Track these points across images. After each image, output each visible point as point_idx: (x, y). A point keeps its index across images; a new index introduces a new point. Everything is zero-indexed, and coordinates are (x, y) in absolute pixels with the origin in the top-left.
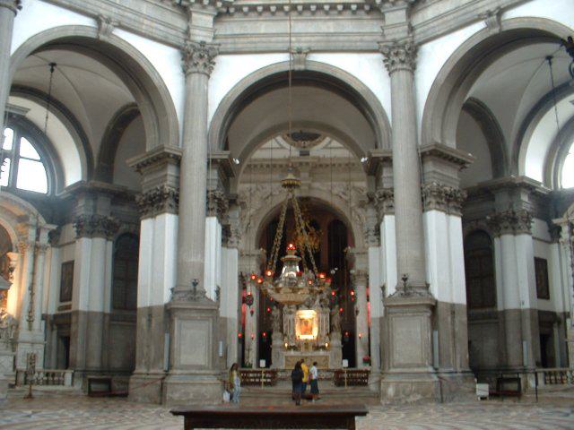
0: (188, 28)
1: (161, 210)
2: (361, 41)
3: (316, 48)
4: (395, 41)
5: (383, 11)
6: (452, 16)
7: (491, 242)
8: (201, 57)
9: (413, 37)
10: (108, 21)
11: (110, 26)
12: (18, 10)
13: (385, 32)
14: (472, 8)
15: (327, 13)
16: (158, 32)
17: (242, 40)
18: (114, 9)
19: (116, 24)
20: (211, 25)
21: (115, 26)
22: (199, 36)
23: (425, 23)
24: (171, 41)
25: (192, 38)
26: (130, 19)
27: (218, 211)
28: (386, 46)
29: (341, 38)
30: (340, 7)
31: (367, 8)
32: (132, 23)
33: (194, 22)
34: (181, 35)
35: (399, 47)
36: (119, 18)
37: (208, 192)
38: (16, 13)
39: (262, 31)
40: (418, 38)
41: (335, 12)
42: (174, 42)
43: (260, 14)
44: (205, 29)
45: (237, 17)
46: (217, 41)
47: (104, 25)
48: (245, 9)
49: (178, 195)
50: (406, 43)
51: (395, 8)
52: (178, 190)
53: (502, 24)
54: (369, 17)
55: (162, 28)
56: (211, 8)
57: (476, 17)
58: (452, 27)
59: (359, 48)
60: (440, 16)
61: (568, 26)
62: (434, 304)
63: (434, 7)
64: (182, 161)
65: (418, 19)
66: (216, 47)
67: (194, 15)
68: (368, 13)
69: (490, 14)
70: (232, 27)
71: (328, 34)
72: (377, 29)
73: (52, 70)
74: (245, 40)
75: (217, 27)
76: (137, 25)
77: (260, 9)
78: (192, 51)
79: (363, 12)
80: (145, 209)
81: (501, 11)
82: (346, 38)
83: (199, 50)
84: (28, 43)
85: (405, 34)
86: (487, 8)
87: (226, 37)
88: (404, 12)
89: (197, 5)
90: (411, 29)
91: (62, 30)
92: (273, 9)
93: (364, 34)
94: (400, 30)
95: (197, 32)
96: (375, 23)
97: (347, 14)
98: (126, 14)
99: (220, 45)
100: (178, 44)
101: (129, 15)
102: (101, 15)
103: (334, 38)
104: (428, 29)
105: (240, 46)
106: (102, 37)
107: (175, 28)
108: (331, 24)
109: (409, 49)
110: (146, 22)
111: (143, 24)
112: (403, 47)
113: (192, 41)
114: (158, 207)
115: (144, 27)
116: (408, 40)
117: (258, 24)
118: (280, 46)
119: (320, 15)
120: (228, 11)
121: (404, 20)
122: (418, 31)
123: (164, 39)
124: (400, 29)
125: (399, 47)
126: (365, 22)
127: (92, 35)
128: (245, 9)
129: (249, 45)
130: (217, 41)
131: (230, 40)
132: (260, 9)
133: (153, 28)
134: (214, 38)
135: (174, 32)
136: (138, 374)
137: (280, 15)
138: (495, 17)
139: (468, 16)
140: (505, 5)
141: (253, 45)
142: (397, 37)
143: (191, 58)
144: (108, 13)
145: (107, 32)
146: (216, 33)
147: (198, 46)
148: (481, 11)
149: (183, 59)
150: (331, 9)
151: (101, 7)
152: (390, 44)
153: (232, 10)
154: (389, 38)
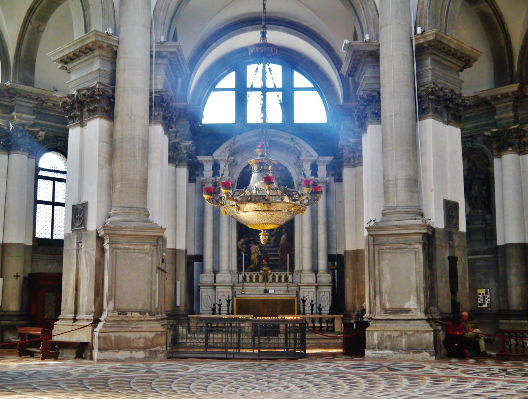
1: (93, 113)
7: (490, 164)
27: (165, 118)
37: (151, 94)
49: (113, 97)
52: (114, 91)
62: (430, 233)
64: (120, 54)
80: (72, 114)
114: (89, 111)
136: (63, 319)
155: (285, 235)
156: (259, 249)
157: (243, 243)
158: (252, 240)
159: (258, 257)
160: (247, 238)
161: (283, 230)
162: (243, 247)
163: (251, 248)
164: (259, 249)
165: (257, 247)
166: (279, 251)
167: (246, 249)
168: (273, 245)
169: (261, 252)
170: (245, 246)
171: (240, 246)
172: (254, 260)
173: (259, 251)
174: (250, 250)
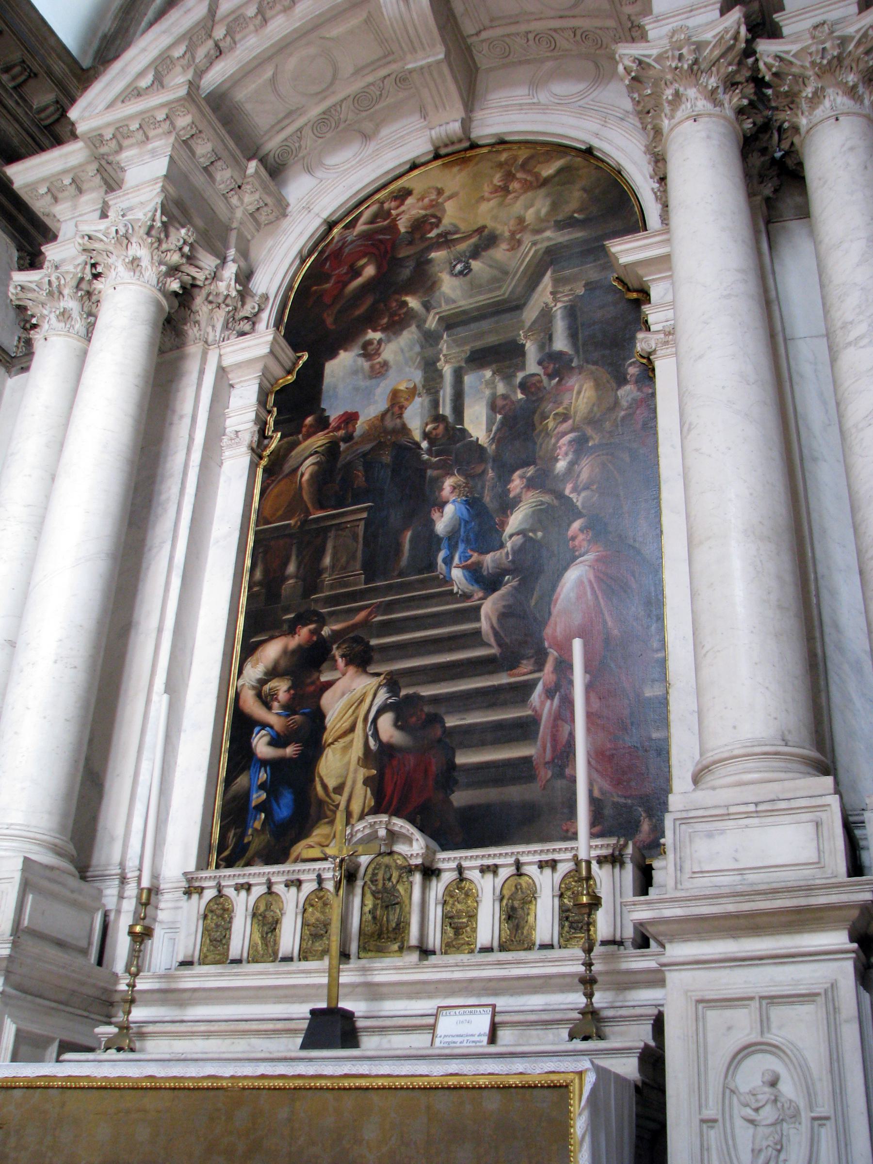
155: (590, 557)
156: (383, 696)
157: (273, 673)
158: (337, 636)
159: (368, 757)
160: (304, 633)
161: (576, 525)
162: (266, 700)
163: (327, 699)
164: (383, 696)
165: (374, 682)
166: (537, 696)
167: (289, 708)
168: (494, 650)
169: (399, 724)
170: (282, 687)
171: (252, 706)
172: (339, 789)
173: (380, 712)
174: (318, 718)
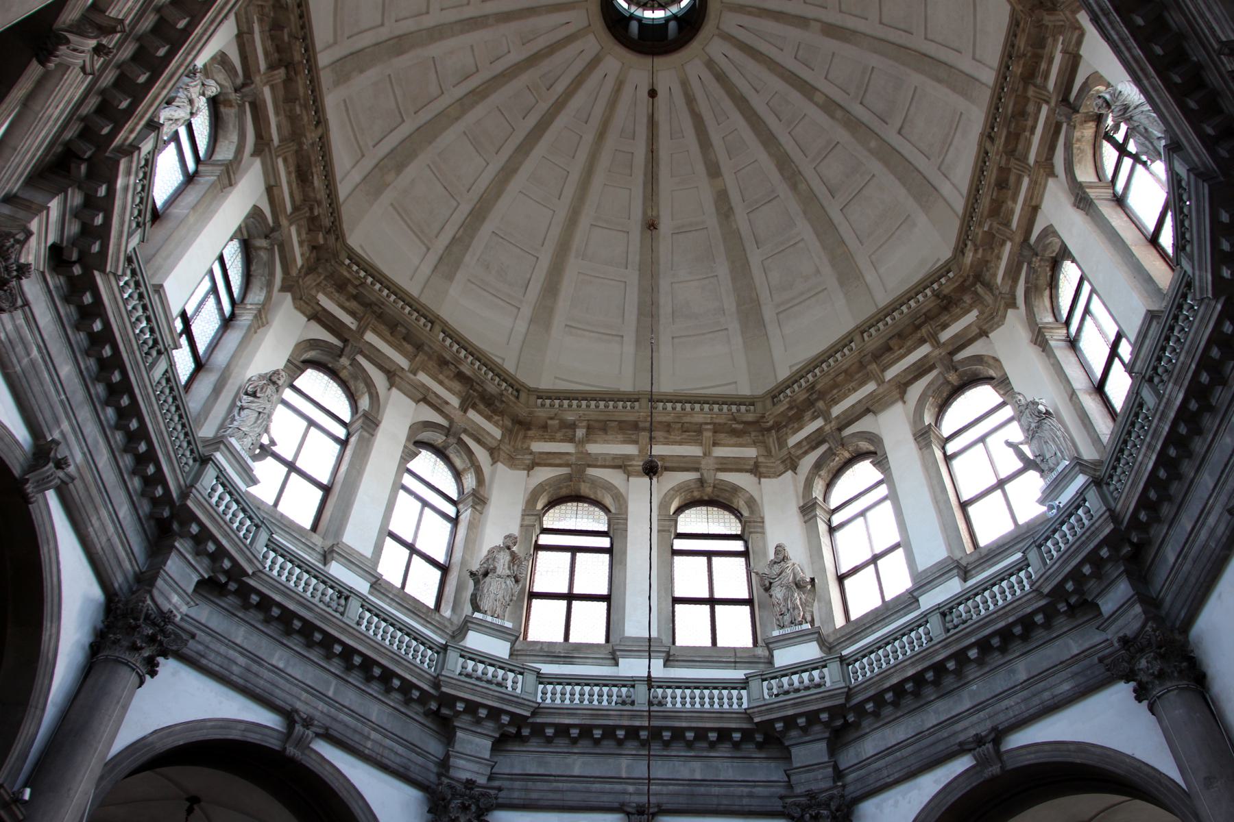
0: (447, 756)
2: (751, 796)
3: (669, 806)
4: (811, 795)
5: (787, 743)
6: (909, 749)
8: (465, 808)
9: (844, 786)
10: (308, 723)
11: (310, 733)
12: (148, 677)
13: (793, 778)
14: (945, 734)
15: (690, 745)
16: (392, 756)
17: (539, 785)
18: (321, 705)
19: (321, 731)
20: (487, 756)
21: (318, 735)
22: (464, 770)
23: (862, 764)
24: (413, 776)
25: (452, 773)
26: (346, 726)
28: (798, 805)
29: (715, 790)
30: (713, 736)
31: (759, 738)
32: (349, 733)
33: (458, 747)
34: (435, 769)
35: (819, 805)
36: (328, 722)
38: (141, 683)
39: (576, 772)
40: (851, 791)
41: (705, 745)
42: (419, 778)
43: (574, 741)
44: (478, 759)
45: (533, 745)
46: (496, 784)
47: (298, 728)
48: (550, 732)
50: (831, 798)
51: (807, 739)
53: (1005, 757)
54: (763, 755)
55: (400, 750)
56: (490, 724)
57: (956, 748)
58: (913, 768)
59: (746, 809)
60: (889, 751)
61: (1129, 752)
63: (877, 735)
65: (848, 758)
66: (492, 792)
67: (459, 734)
68: (760, 746)
69: (979, 741)
70: (522, 761)
71: (692, 782)
72: (778, 775)
73: (190, 811)
74: (545, 786)
75: (499, 759)
76: (357, 738)
77: (574, 732)
78: (449, 797)
79: (751, 746)
81: (999, 735)
82: (723, 790)
83: (462, 796)
84: (150, 739)
85: (829, 784)
86: (972, 732)
87: (513, 777)
88: (823, 746)
89: (467, 718)
90: (839, 774)
91: (221, 727)
92: (597, 733)
93: (755, 783)
94: (820, 777)
95: (461, 763)
96: (773, 764)
97: (724, 750)
98: (342, 716)
99: (500, 789)
100: (427, 783)
101: (347, 719)
102: (297, 711)
103: (702, 790)
104: (869, 774)
105: (534, 795)
106: (291, 751)
107: (423, 753)
108: (697, 765)
109: (837, 810)
110: (374, 735)
111: (368, 738)
112: (828, 806)
113: (452, 779)
115: (369, 744)
116: (835, 792)
117: (570, 759)
118: (606, 800)
119: (677, 750)
120: (519, 732)
121: (826, 759)
122: (851, 777)
123: (402, 770)
124: (819, 774)
125: (819, 805)
126: (756, 763)
127: (274, 744)
128: (550, 732)
129: (551, 796)
130: (496, 784)
131: (517, 784)
132: (574, 732)
133: (385, 747)
134: (490, 778)
135: (420, 760)
137: (608, 745)
138: (990, 746)
139: (941, 747)
140: (1006, 724)
141: (558, 796)
142: (814, 787)
143: (446, 807)
144: (310, 711)
145: (302, 744)
146: (494, 771)
147: (459, 787)
148: (962, 737)
149: (429, 811)
150: (696, 738)
151: (300, 699)
152: (803, 800)
153: (526, 732)
154: (799, 790)
